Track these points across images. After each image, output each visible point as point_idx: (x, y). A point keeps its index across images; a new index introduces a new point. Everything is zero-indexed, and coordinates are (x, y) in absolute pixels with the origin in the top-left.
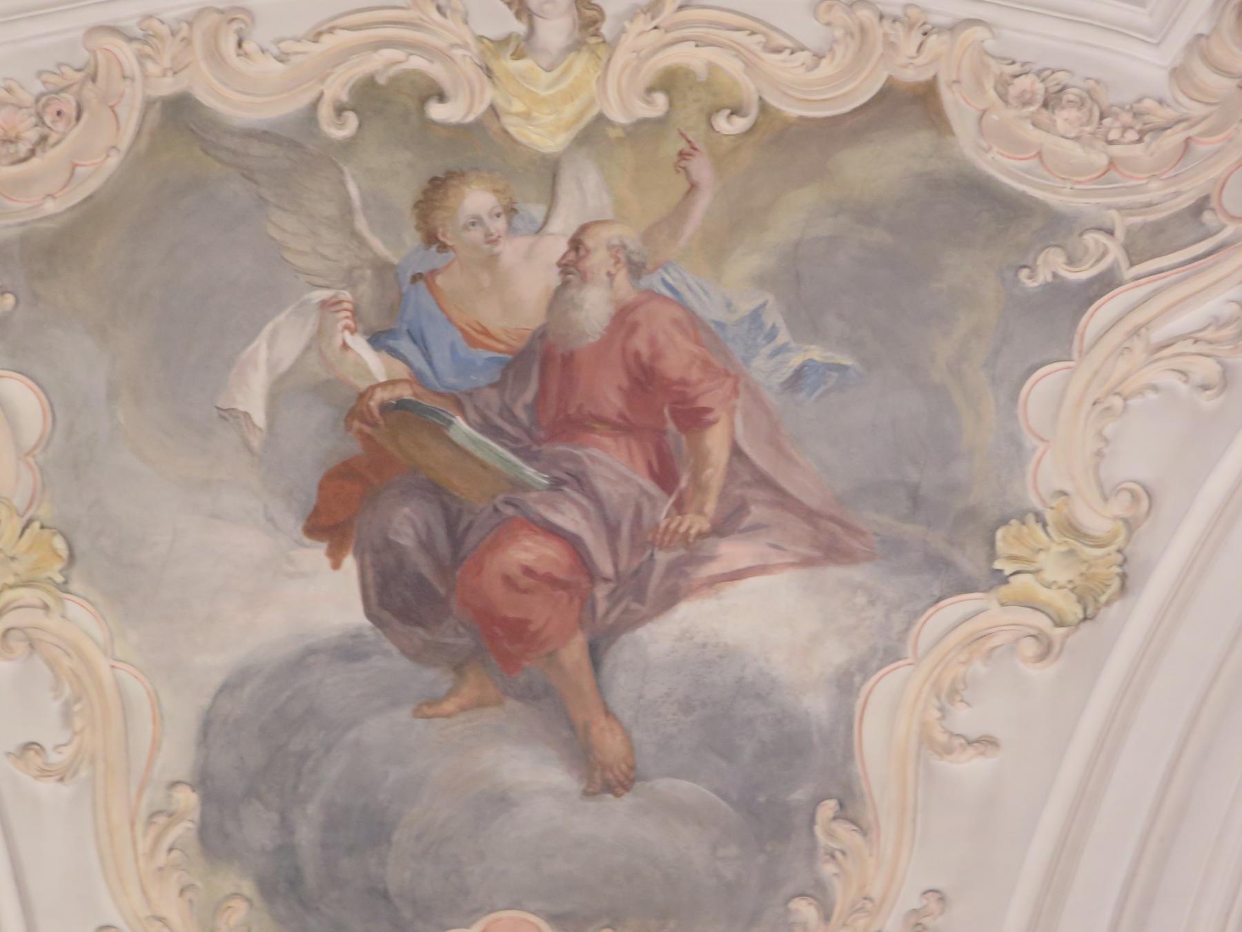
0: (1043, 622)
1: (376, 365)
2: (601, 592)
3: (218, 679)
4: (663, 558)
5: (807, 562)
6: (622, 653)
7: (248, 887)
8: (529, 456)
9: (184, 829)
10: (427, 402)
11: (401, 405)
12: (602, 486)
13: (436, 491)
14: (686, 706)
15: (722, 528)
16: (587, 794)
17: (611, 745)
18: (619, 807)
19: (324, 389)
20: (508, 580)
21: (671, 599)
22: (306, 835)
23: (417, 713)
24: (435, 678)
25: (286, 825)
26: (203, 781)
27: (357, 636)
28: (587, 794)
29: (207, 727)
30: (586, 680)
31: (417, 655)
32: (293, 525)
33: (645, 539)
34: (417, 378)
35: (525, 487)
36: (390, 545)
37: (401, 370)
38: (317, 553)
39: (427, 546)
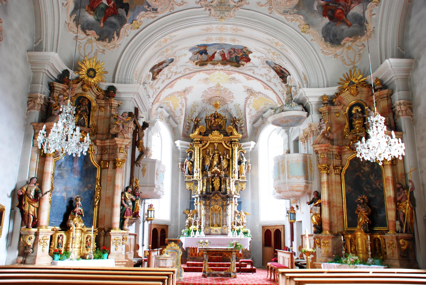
0: (376, 3)
1: (323, 2)
2: (344, 12)
3: (322, 29)
4: (348, 8)
5: (358, 4)
6: (347, 16)
7: (329, 43)
8: (336, 4)
9: (323, 41)
10: (328, 3)
11: (326, 4)
12: (342, 4)
13: (330, 10)
14: (353, 18)
15: (351, 4)
16: (349, 27)
17: (349, 23)
18: (351, 27)
19: (320, 6)
20: (338, 14)
21: (349, 11)
22: (331, 37)
23: (335, 26)
24: (336, 23)
25: (330, 37)
26: (324, 37)
27: (329, 22)
28: (349, 27)
29: (322, 33)
30: (346, 19)
31: (334, 22)
32: (322, 16)
33: (346, 7)
34: (326, 2)
35: (336, 6)
36: (329, 15)
37: (325, 2)
38: (324, 18)
39: (331, 14)
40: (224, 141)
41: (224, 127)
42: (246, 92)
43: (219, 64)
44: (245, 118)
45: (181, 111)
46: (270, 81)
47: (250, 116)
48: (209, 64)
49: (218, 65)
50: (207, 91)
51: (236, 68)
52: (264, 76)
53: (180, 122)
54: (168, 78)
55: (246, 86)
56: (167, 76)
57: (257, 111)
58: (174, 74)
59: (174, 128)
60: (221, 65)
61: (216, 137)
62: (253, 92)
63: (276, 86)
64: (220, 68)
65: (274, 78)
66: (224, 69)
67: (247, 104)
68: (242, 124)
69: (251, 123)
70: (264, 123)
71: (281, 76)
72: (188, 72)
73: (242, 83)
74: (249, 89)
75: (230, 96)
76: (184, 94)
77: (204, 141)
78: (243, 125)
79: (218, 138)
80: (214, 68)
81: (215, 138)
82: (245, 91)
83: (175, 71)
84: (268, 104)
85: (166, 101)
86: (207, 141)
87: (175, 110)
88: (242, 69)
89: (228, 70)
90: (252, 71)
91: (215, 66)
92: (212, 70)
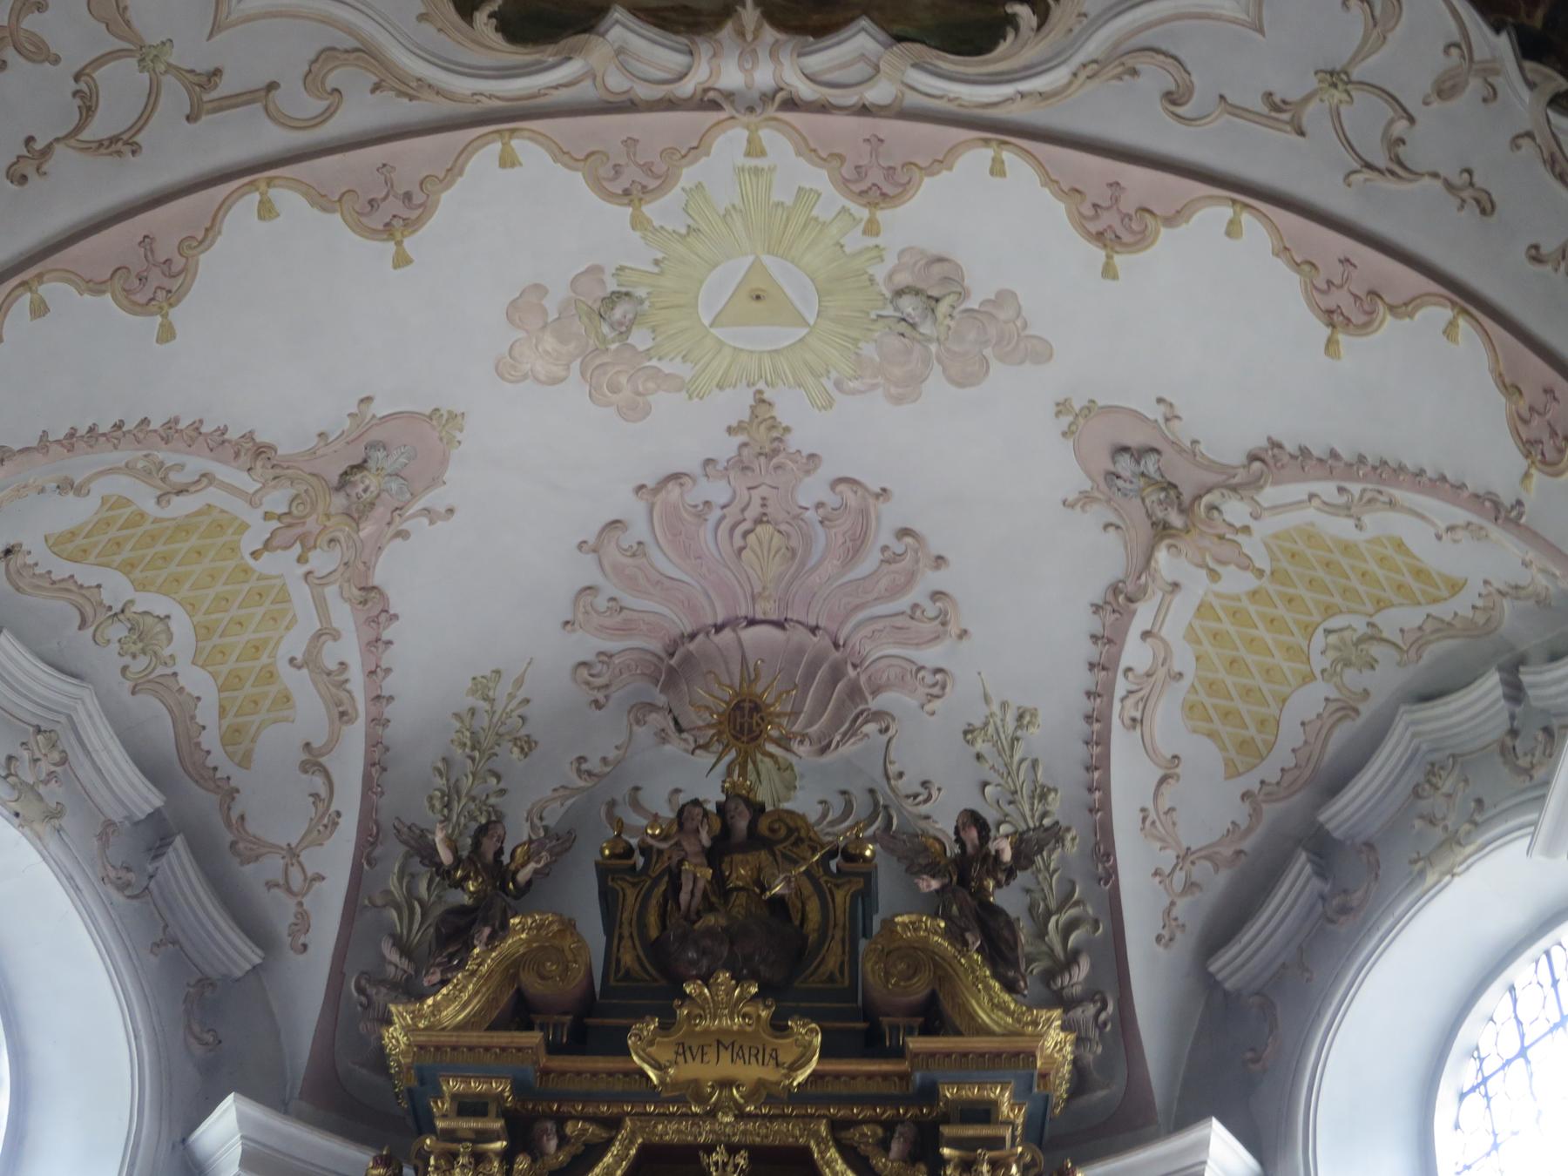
40: (836, 1126)
41: (833, 958)
42: (1099, 513)
43: (750, 15)
44: (1111, 875)
45: (319, 783)
46: (1399, 168)
47: (1168, 859)
48: (618, 13)
49: (727, 32)
50: (639, 530)
51: (949, 62)
52: (1313, 114)
53: (303, 922)
54: (98, 129)
55: (1090, 409)
56: (88, 108)
57: (1251, 782)
58: (174, 97)
59: (205, 982)
60: (770, 34)
61: (725, 1066)
62: (1187, 478)
63: (1486, 207)
64: (764, 76)
65: (1445, 89)
66: (806, 91)
67: (1121, 686)
68: (1072, 958)
69: (1185, 943)
70: (1345, 910)
71: (1538, 21)
72: (360, 112)
73: (1041, 353)
74: (1135, 439)
75: (903, 603)
76: (355, 515)
77: (561, 1120)
78: (1082, 971)
79: (751, 1072)
80: (687, 88)
81: (707, 1069)
82: (1086, 499)
83: (192, 53)
84: (1374, 636)
85: (116, 587)
86: (613, 1124)
87: (245, 762)
88: (1028, 72)
89: (864, 110)
90: (1154, 78)
91: (704, 48)
92: (670, 104)
